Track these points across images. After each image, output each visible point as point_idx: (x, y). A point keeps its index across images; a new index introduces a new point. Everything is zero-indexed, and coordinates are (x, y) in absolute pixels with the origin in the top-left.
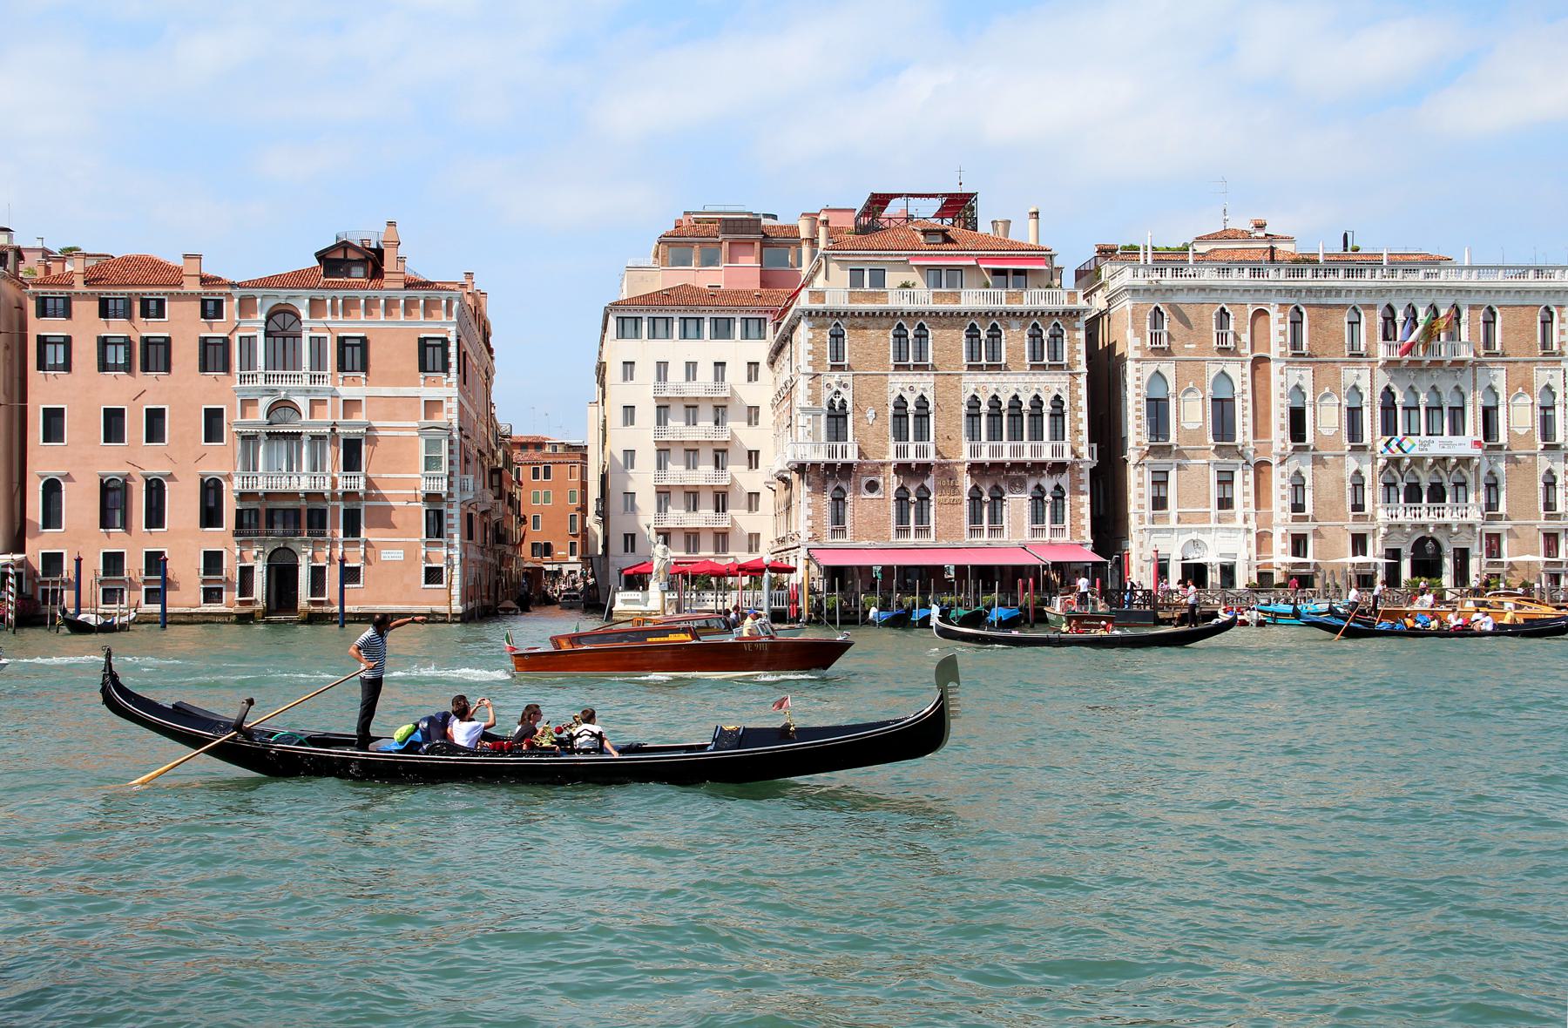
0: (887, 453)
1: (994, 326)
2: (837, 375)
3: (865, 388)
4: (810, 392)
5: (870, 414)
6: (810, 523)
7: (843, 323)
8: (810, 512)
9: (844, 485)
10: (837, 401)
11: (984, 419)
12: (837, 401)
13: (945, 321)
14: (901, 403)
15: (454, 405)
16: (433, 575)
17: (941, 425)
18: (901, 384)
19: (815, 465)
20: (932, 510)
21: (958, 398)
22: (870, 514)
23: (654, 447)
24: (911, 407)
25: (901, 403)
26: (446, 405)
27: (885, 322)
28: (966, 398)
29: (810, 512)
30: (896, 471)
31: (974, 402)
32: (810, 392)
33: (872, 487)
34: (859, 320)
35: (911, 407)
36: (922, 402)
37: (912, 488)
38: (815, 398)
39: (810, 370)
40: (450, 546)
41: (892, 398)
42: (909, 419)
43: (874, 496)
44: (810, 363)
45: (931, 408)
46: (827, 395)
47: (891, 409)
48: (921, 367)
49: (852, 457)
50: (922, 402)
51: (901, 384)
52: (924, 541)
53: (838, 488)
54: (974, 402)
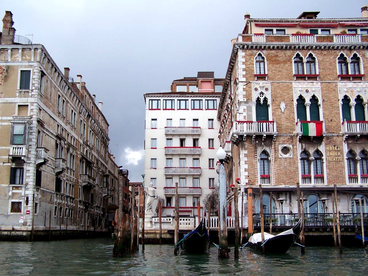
0: (294, 130)
1: (355, 55)
2: (261, 83)
3: (278, 91)
4: (244, 93)
5: (283, 106)
6: (247, 174)
7: (264, 53)
8: (246, 166)
9: (268, 150)
10: (262, 99)
11: (353, 111)
12: (262, 99)
13: (325, 52)
14: (301, 99)
15: (35, 107)
16: (16, 207)
17: (327, 113)
18: (300, 88)
19: (249, 136)
20: (325, 165)
21: (336, 97)
22: (285, 167)
23: (165, 157)
24: (308, 102)
25: (301, 99)
26: (30, 108)
27: (288, 53)
28: (341, 97)
29: (246, 166)
30: (300, 141)
31: (346, 100)
32: (244, 93)
33: (286, 150)
34: (273, 52)
35: (308, 102)
36: (314, 99)
37: (311, 151)
38: (248, 97)
39: (244, 79)
40: (26, 189)
41: (296, 98)
42: (307, 109)
43: (287, 156)
44: (244, 76)
45: (320, 102)
46: (255, 95)
47: (295, 103)
48: (313, 77)
49: (273, 131)
50: (314, 99)
51: (300, 88)
52: (320, 185)
53: (264, 152)
54: (346, 100)
